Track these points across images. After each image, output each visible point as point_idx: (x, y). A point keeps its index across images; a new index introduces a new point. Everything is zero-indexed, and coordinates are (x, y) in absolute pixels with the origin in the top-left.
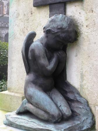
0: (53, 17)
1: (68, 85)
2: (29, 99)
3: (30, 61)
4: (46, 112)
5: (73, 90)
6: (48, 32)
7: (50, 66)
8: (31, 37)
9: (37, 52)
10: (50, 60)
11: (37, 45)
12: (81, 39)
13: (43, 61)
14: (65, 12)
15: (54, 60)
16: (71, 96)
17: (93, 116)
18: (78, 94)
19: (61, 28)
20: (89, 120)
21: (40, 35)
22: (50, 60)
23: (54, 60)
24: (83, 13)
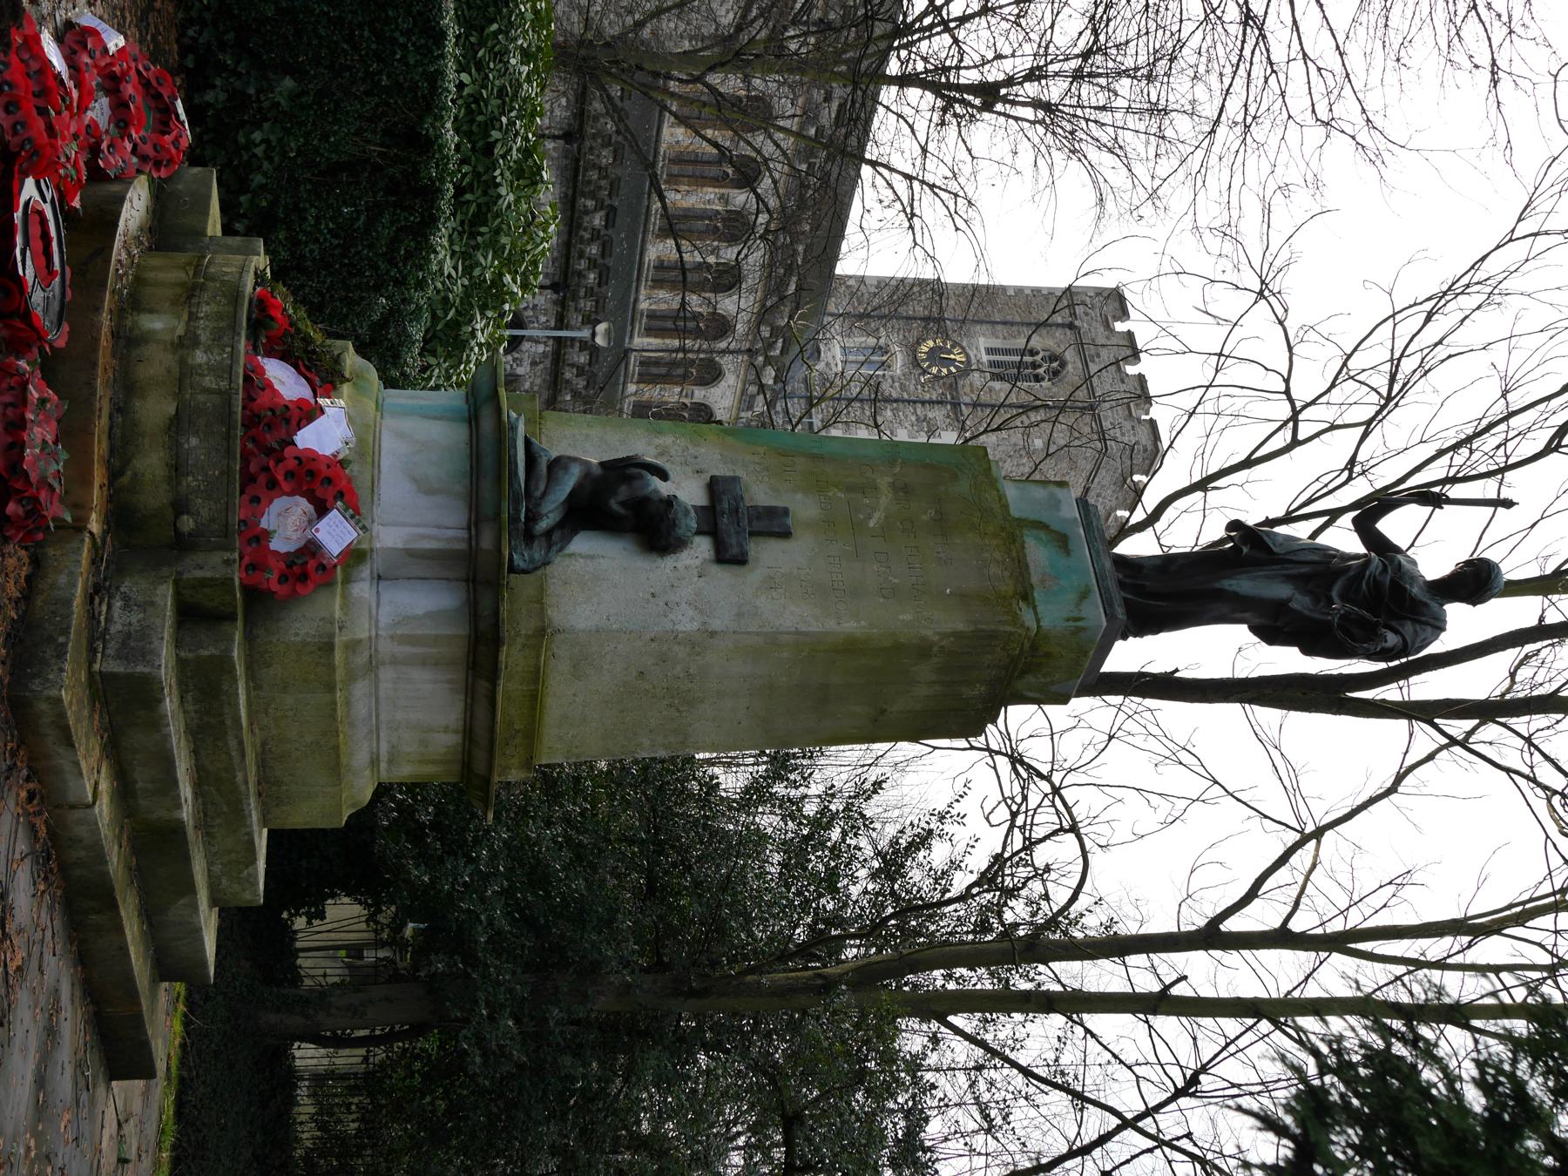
0: (693, 514)
1: (575, 532)
2: (558, 465)
3: (624, 470)
4: (544, 494)
5: (566, 540)
6: (670, 502)
7: (614, 505)
8: (664, 476)
9: (637, 483)
10: (623, 504)
11: (648, 485)
12: (654, 556)
13: (623, 492)
14: (699, 533)
15: (622, 511)
16: (556, 536)
17: (525, 572)
18: (561, 550)
19: (675, 525)
20: (522, 565)
21: (664, 488)
22: (623, 504)
23: (622, 511)
24: (698, 562)
